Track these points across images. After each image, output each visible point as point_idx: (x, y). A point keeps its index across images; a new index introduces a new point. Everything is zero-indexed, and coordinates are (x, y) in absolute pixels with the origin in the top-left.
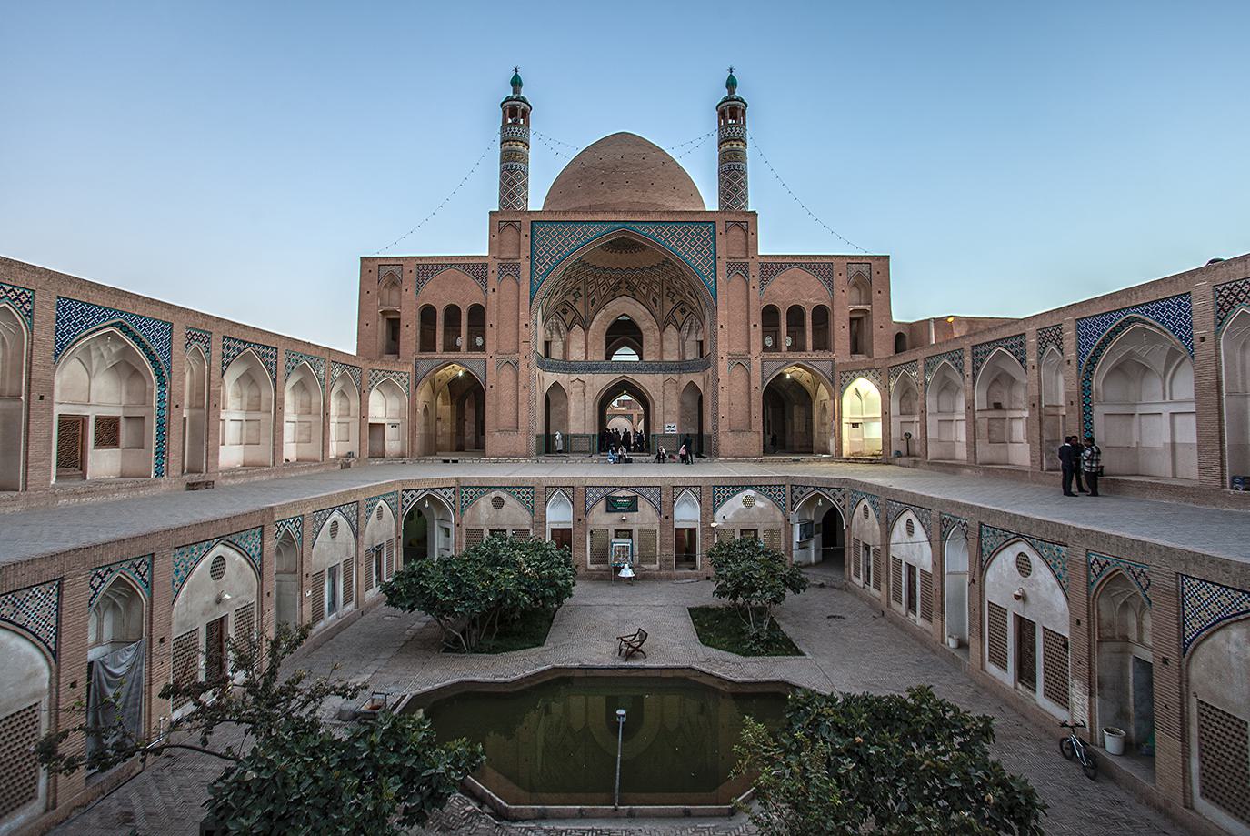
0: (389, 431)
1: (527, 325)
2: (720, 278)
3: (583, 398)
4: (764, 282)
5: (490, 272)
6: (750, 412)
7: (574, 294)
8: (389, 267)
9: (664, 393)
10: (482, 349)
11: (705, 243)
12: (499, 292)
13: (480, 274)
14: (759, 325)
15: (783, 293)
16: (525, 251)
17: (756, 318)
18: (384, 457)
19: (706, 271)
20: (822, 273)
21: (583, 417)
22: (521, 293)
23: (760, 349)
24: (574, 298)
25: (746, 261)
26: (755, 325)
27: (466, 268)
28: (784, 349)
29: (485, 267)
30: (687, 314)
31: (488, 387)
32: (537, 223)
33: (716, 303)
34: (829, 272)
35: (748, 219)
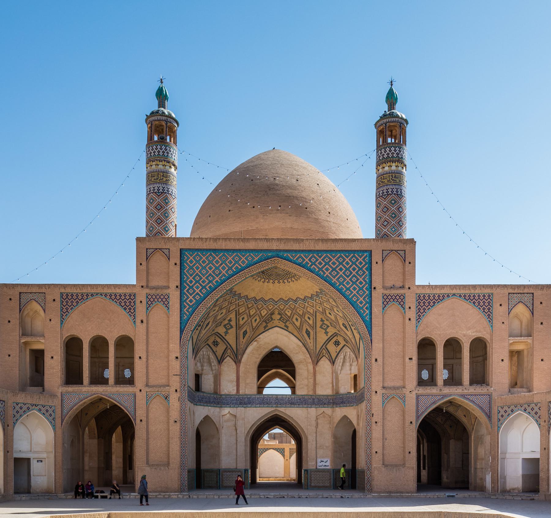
0: (35, 467)
1: (177, 358)
2: (375, 310)
3: (234, 433)
4: (420, 314)
5: (138, 302)
6: (404, 447)
7: (225, 326)
8: (30, 295)
9: (317, 427)
10: (131, 382)
11: (361, 273)
12: (147, 323)
13: (128, 304)
14: (415, 358)
15: (441, 325)
16: (175, 281)
17: (413, 351)
18: (29, 492)
19: (361, 303)
20: (482, 304)
21: (235, 451)
22: (171, 325)
23: (415, 382)
24: (225, 330)
25: (401, 291)
26: (411, 359)
27: (113, 297)
28: (440, 382)
29: (132, 297)
30: (341, 346)
31: (138, 421)
32: (186, 253)
33: (371, 335)
34: (489, 303)
35: (407, 248)
